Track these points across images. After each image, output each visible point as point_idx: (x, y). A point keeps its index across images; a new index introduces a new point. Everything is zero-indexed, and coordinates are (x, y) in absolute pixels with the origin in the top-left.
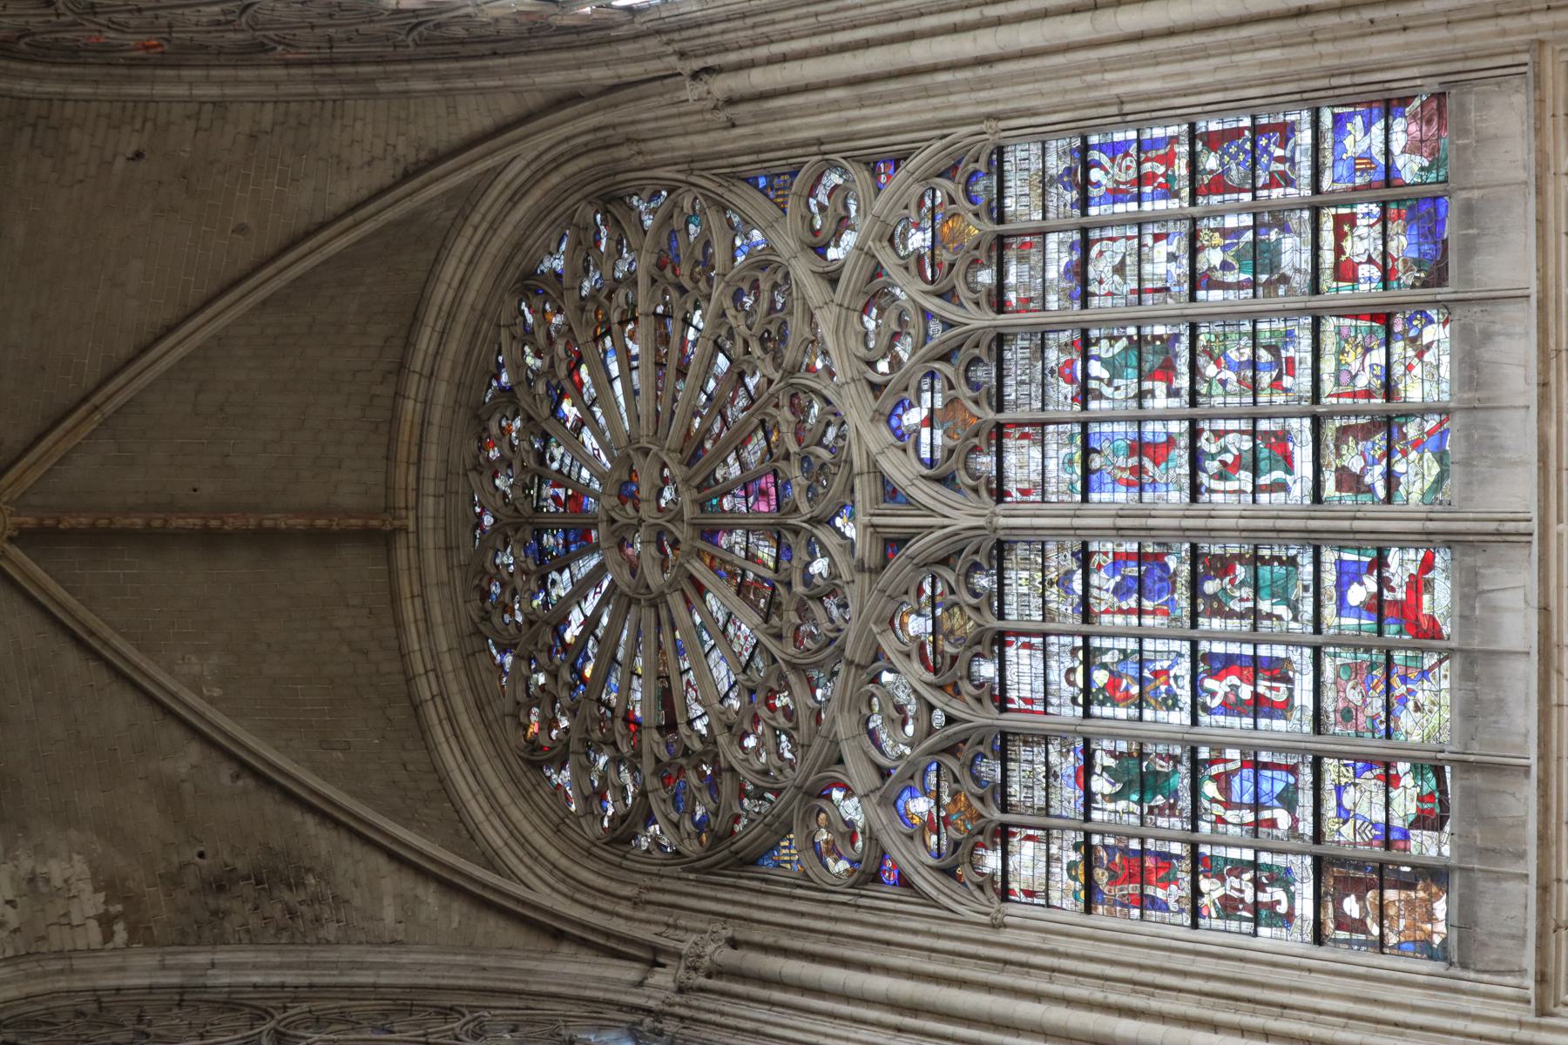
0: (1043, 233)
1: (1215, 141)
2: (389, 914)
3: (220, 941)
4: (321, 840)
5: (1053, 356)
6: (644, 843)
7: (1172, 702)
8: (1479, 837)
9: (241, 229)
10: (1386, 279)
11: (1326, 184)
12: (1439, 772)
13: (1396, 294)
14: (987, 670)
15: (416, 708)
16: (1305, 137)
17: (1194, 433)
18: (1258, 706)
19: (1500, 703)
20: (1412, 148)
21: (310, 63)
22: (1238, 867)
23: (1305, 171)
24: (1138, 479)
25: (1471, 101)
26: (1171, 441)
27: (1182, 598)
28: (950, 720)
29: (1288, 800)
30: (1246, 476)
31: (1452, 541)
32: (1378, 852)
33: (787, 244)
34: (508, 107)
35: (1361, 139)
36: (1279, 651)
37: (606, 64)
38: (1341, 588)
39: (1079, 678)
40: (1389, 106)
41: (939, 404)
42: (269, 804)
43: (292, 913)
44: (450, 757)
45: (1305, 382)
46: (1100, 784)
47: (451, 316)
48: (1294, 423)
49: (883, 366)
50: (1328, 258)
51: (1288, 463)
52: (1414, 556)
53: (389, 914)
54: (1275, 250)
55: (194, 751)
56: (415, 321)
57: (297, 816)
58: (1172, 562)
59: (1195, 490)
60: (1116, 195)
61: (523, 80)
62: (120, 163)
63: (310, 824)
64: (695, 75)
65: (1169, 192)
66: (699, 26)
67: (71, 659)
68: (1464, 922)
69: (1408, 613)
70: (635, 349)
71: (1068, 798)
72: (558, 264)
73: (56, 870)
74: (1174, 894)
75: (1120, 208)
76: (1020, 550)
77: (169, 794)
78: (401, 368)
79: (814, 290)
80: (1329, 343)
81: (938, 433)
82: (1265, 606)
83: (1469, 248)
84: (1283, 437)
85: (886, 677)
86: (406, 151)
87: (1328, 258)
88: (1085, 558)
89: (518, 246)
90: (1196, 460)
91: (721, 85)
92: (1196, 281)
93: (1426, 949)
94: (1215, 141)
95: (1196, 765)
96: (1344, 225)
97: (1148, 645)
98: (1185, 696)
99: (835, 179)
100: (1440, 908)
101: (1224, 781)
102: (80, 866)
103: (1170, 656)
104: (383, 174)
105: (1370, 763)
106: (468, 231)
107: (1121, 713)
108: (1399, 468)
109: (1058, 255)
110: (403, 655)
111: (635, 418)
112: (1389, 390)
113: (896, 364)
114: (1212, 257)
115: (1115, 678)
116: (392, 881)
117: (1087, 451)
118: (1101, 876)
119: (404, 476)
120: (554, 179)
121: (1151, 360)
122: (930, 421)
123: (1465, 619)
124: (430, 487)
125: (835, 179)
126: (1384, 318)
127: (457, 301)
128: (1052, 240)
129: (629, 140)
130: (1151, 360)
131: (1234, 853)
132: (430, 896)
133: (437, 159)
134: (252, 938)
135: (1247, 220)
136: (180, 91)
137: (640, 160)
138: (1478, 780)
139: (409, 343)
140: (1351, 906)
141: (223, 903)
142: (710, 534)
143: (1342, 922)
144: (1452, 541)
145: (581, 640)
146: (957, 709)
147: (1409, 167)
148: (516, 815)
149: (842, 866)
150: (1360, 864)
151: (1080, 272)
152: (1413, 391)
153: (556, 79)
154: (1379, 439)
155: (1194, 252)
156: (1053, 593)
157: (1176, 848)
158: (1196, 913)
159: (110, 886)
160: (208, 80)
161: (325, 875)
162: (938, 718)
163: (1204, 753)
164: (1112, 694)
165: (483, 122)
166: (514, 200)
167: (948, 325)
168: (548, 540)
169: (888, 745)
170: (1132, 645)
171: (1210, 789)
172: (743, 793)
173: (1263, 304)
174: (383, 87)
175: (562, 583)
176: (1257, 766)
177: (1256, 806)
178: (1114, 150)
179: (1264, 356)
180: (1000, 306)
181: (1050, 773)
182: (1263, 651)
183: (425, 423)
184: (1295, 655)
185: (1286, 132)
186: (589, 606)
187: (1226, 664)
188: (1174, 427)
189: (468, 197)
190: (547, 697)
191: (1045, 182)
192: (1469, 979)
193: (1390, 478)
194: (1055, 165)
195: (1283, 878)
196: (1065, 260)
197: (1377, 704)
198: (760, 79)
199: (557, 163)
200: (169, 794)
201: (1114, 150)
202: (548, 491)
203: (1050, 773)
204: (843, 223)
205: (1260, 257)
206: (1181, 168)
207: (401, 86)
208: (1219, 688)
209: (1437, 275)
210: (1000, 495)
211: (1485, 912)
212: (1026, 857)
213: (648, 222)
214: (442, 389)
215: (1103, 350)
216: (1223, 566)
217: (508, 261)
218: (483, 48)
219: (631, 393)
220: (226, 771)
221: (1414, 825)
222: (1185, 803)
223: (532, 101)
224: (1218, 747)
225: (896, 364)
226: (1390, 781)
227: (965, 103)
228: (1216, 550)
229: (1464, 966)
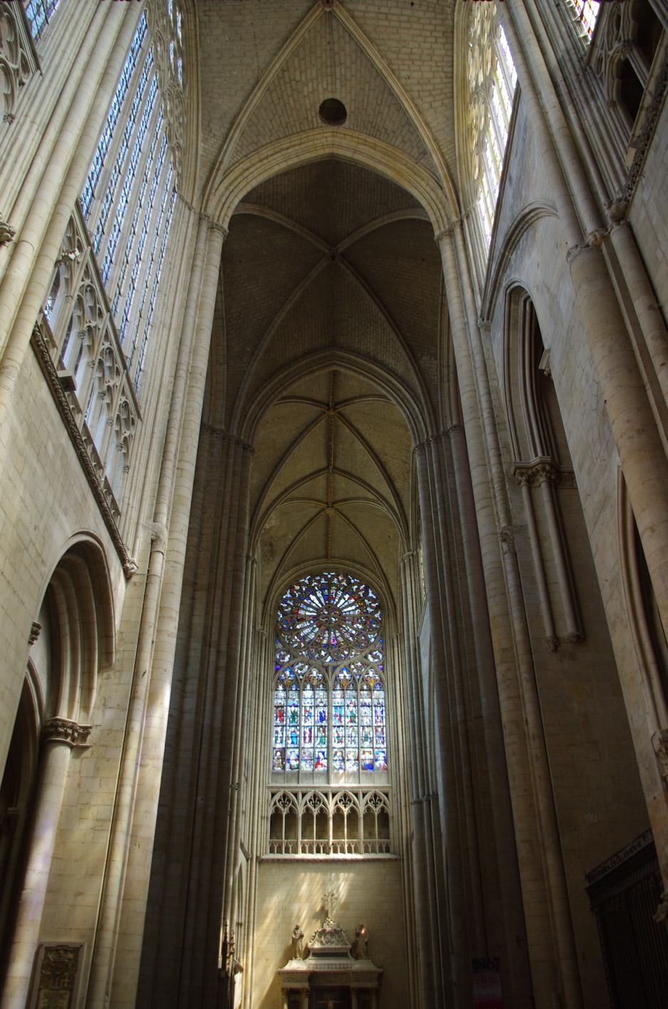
0: (371, 698)
1: (382, 730)
2: (267, 572)
3: (261, 546)
4: (278, 559)
5: (353, 700)
6: (279, 613)
7: (305, 722)
8: (290, 775)
9: (377, 548)
10: (363, 760)
11: (376, 750)
12: (298, 768)
13: (360, 761)
14: (308, 687)
15: (298, 564)
16: (382, 746)
17: (342, 726)
18: (305, 738)
19: (307, 779)
20: (380, 765)
22: (282, 734)
23: (378, 746)
24: (336, 716)
25: (386, 775)
26: (341, 722)
27: (320, 724)
28: (301, 680)
29: (292, 743)
30: (336, 735)
31: (328, 770)
32: (286, 758)
33: (371, 648)
34: (395, 596)
35: (381, 756)
36: (313, 741)
38: (322, 752)
39: (308, 705)
40: (386, 760)
41: (347, 678)
42: (284, 550)
43: (266, 556)
44: (290, 572)
45: (349, 746)
46: (293, 708)
48: (343, 744)
49: (352, 667)
50: (366, 750)
51: (338, 742)
52: (326, 764)
53: (267, 572)
54: (367, 741)
55: (292, 538)
56: (362, 565)
57: (282, 554)
58: (324, 722)
59: (335, 727)
60: (376, 712)
63: (281, 557)
65: (376, 722)
67: (307, 520)
68: (277, 773)
69: (318, 763)
70: (357, 611)
71: (290, 702)
72: (371, 595)
73: (273, 521)
74: (278, 721)
75: (374, 712)
76: (326, 694)
77: (285, 535)
78: (354, 561)
79: (364, 654)
80: (354, 750)
81: (342, 678)
82: (319, 739)
83: (366, 774)
84: (342, 742)
85: (307, 667)
86: (388, 576)
87: (366, 750)
88: (325, 706)
90: (339, 727)
91: (395, 641)
92: (363, 726)
93: (274, 766)
94: (382, 730)
95: (296, 726)
96: (370, 752)
97: (313, 718)
98: (306, 725)
99: (381, 657)
100: (279, 769)
101: (294, 731)
102: (274, 524)
103: (310, 722)
105: (298, 756)
107: (303, 713)
108: (338, 762)
109: (368, 701)
110: (307, 561)
111: (345, 612)
112: (348, 760)
113: (353, 669)
114: (366, 729)
115: (308, 712)
116: (271, 572)
117: (340, 707)
118: (280, 709)
119: (337, 561)
121: (352, 718)
122: (345, 676)
123: (318, 773)
124: (335, 565)
125: (381, 657)
126: (358, 759)
128: (370, 700)
130: (352, 718)
131: (284, 733)
132: (270, 578)
134: (262, 551)
135: (371, 736)
138: (297, 775)
139: (358, 563)
140: (279, 754)
141: (268, 545)
142: (328, 629)
143: (276, 752)
144: (328, 770)
145: (310, 599)
146: (303, 681)
147: (377, 764)
148: (282, 586)
149: (278, 657)
150: (284, 755)
151: (364, 705)
152: (348, 764)
154: (341, 758)
155: (367, 726)
156: (319, 700)
157: (285, 722)
158: (276, 726)
159: (271, 529)
161: (273, 560)
162: (301, 677)
163: (298, 728)
164: (306, 711)
167: (358, 680)
168: (326, 591)
169: (298, 666)
170: (313, 714)
171: (293, 729)
172: (288, 636)
173: (360, 738)
175: (319, 595)
176: (297, 737)
177: (291, 737)
178: (382, 712)
179: (353, 739)
180: (361, 690)
181: (294, 699)
182: (313, 738)
183: (345, 565)
184: (312, 743)
185: (383, 743)
186: (316, 601)
187: (310, 731)
188: (343, 722)
190: (301, 589)
191: (378, 699)
192: (271, 774)
193: (336, 760)
194: (381, 701)
195: (282, 742)
196: (367, 703)
197: (306, 758)
198: (396, 649)
200: (285, 535)
201: (382, 712)
202: (334, 591)
203: (294, 699)
204: (374, 658)
205: (366, 738)
206: (379, 724)
208: (307, 730)
209: (363, 769)
210: (334, 690)
211: (280, 777)
212: (282, 694)
213: (376, 616)
215: (354, 709)
216: (324, 732)
219: (349, 611)
220: (289, 543)
221: (290, 765)
222: (291, 725)
223: (396, 601)
224: (299, 730)
225: (353, 669)
226: (296, 760)
227: (390, 686)
228: (326, 730)
229: (273, 773)
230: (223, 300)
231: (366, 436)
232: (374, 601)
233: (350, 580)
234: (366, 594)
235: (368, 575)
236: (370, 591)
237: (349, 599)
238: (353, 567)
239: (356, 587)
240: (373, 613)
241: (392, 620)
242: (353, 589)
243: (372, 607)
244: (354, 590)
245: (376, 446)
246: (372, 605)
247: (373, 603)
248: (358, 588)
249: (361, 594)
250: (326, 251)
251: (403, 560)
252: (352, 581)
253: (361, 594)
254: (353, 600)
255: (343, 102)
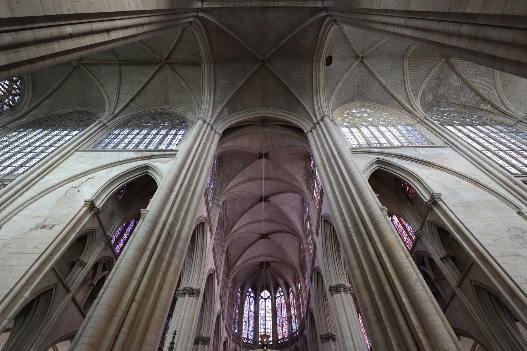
9: (57, 96)
21: (54, 115)
34: (29, 115)
37: (17, 123)
47: (28, 89)
61: (28, 119)
62: (72, 101)
64: (4, 126)
66: (6, 132)
72: (16, 98)
78: (33, 82)
89: (23, 98)
104: (42, 104)
106: (30, 99)
120: (20, 108)
127: (28, 91)
129: (11, 115)
133: (36, 107)
136: (68, 110)
137: (9, 113)
153: (23, 120)
160: (65, 111)
165: (31, 113)
166: (25, 104)
174: (45, 114)
189: (31, 102)
199: (20, 109)
207: (43, 115)
213: (5, 106)
214: (26, 80)
217: (23, 96)
218: (33, 122)
230: (247, 6)
231: (152, 82)
232: (14, 101)
233: (18, 81)
234: (14, 95)
235: (28, 93)
236: (18, 97)
237: (6, 84)
238: (28, 81)
239: (16, 87)
240: (6, 104)
241: (10, 119)
242: (14, 85)
243: (9, 102)
244: (14, 86)
245: (148, 88)
246: (11, 102)
247: (12, 101)
248: (16, 89)
249: (13, 92)
250: (266, 58)
251: (101, 121)
252: (18, 83)
253: (13, 92)
254: (7, 87)
255: (332, 65)
